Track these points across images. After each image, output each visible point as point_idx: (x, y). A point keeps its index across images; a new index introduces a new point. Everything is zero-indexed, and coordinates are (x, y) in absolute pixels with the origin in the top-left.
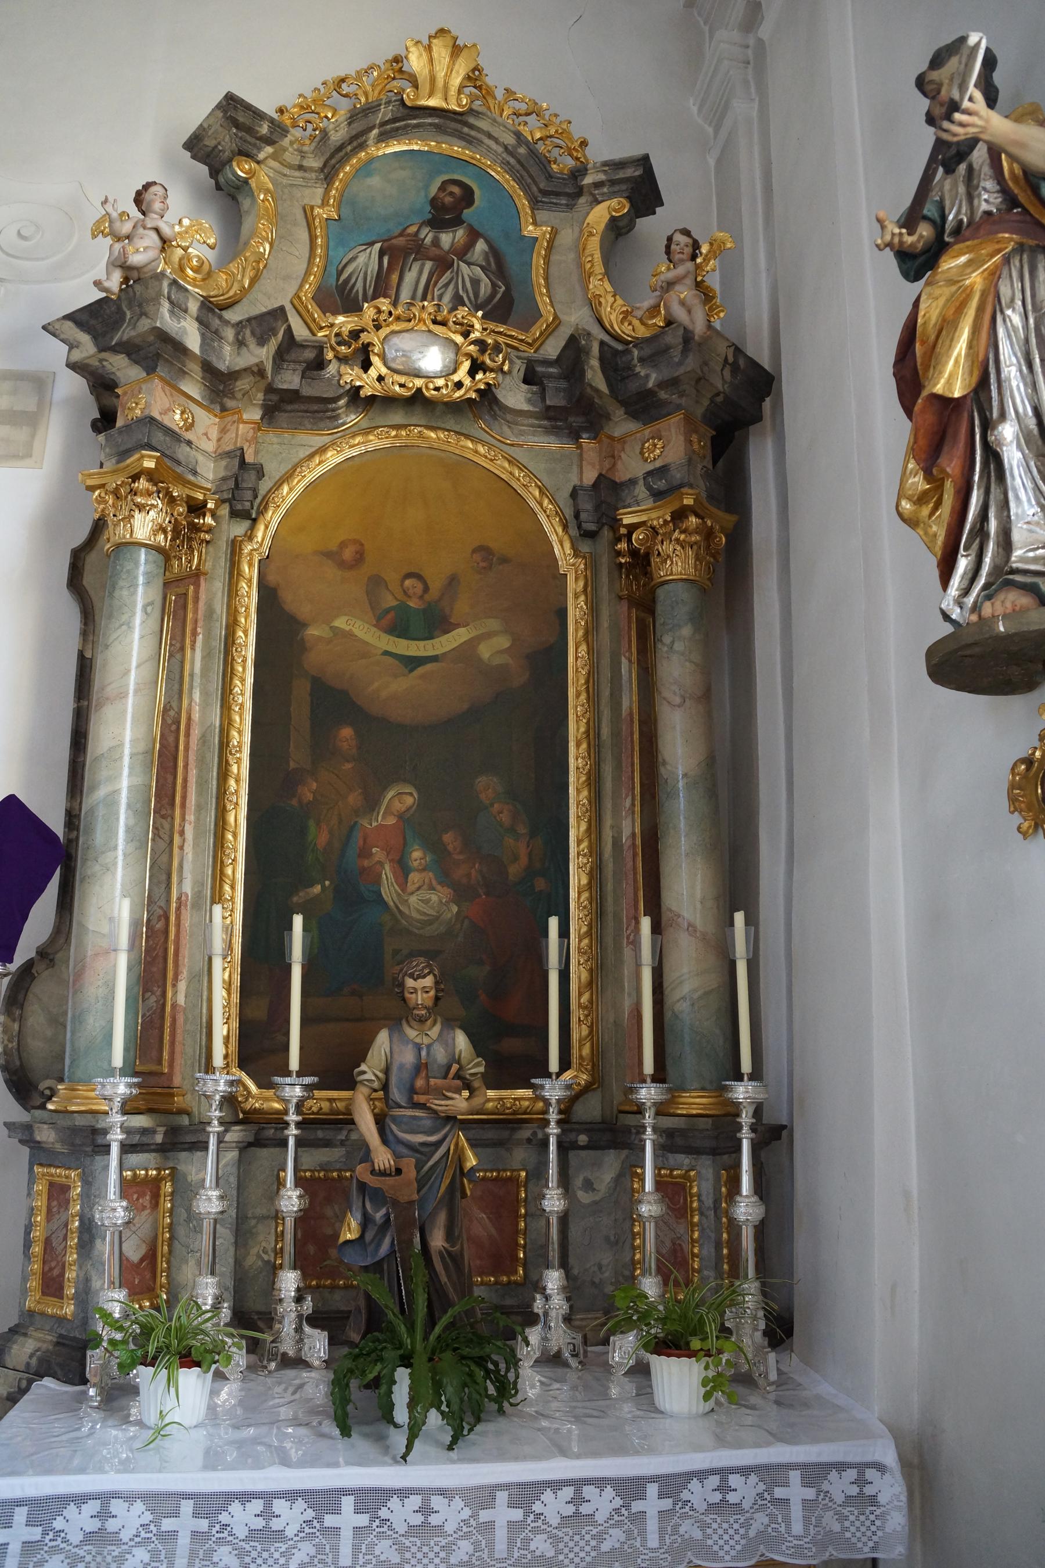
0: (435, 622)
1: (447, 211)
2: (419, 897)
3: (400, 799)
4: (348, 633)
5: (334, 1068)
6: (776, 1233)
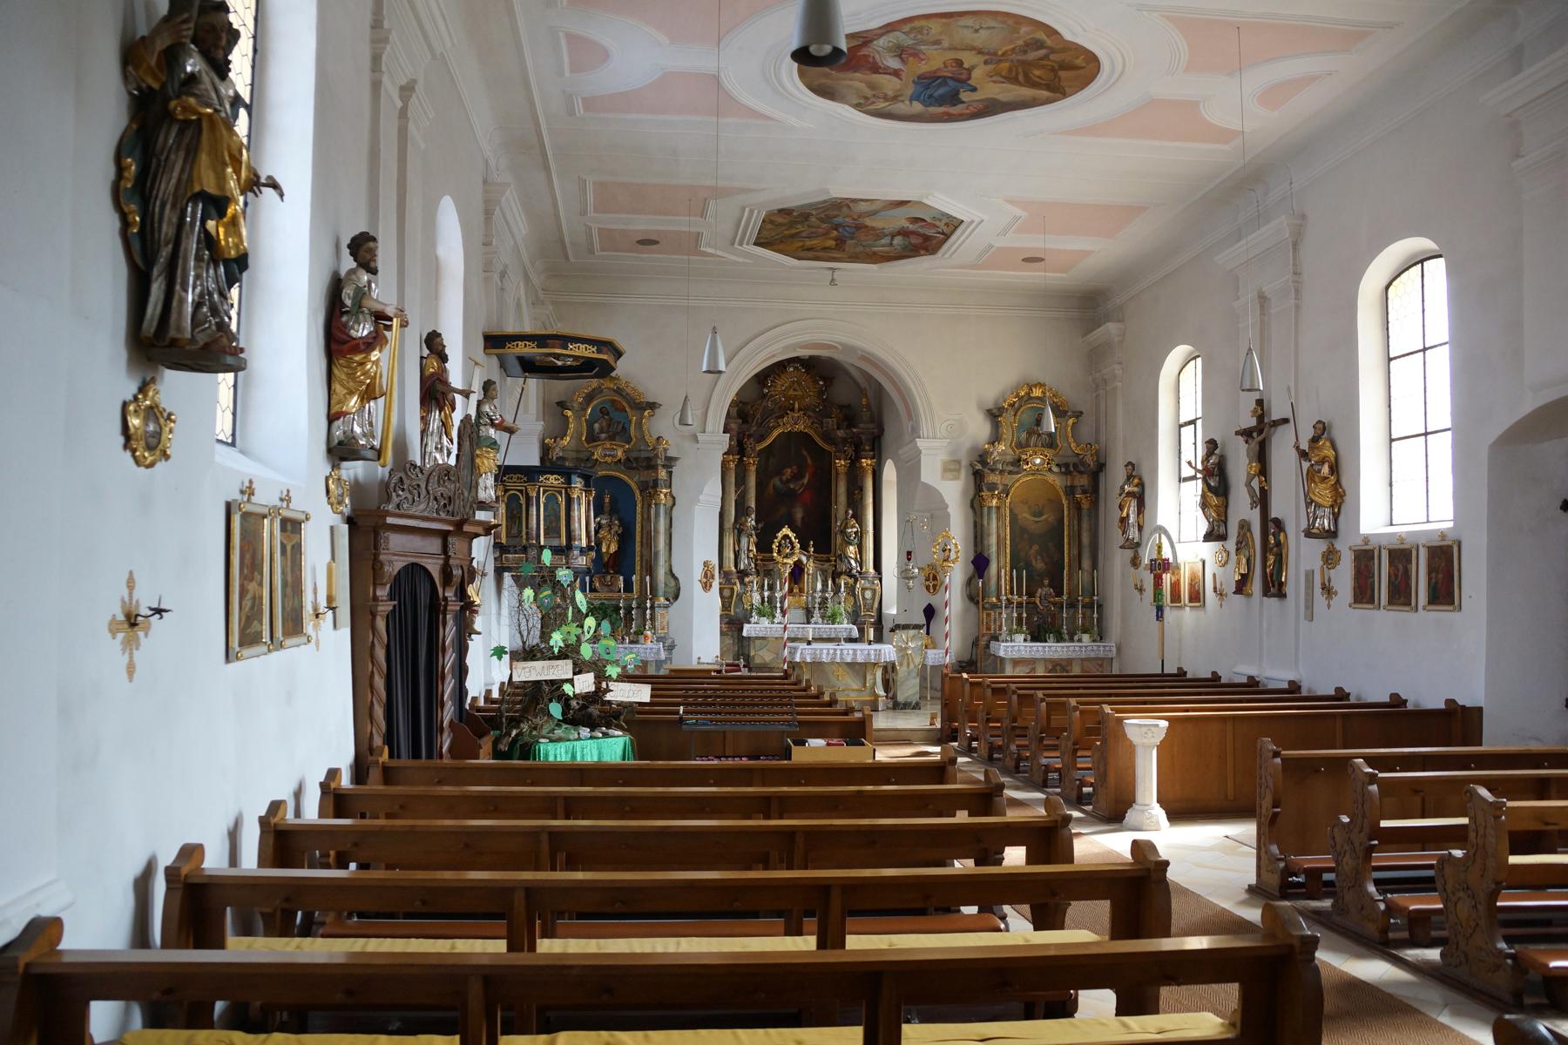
0: (1041, 514)
2: (1039, 565)
3: (1036, 547)
4: (1025, 516)
5: (1030, 594)
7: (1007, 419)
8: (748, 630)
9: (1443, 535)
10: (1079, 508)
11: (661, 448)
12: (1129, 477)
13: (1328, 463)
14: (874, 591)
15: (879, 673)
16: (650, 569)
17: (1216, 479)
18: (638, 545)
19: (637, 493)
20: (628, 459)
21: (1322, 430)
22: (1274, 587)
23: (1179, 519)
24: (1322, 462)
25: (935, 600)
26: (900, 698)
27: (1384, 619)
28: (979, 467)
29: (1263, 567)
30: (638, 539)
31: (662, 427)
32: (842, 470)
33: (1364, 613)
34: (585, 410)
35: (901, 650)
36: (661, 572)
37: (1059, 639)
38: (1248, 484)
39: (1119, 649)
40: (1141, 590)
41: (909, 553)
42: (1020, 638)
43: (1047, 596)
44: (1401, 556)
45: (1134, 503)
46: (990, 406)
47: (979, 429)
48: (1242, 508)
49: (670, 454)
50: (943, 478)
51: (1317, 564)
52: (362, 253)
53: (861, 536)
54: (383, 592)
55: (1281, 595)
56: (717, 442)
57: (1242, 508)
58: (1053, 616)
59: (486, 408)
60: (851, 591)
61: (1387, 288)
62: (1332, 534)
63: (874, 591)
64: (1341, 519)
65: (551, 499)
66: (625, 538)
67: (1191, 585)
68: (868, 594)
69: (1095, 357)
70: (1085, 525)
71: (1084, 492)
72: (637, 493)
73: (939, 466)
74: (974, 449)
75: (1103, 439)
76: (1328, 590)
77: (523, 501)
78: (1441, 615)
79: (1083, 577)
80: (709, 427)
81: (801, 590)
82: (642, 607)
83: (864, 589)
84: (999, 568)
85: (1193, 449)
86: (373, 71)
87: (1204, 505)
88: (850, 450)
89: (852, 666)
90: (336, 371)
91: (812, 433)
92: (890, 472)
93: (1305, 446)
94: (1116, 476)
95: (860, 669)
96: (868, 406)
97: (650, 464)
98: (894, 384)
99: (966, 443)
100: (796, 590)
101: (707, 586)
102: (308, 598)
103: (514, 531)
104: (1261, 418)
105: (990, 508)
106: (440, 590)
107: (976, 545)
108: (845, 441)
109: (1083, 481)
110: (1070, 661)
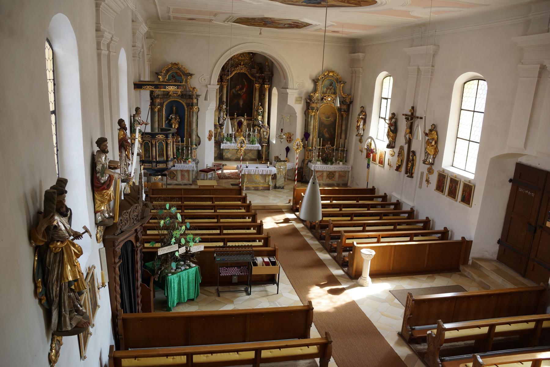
0: (329, 118)
1: (331, 85)
2: (327, 135)
3: (326, 129)
4: (324, 118)
6: (346, 156)
7: (320, 83)
8: (223, 146)
9: (470, 181)
10: (342, 116)
11: (194, 92)
12: (362, 112)
13: (435, 139)
14: (267, 132)
15: (270, 177)
16: (190, 136)
17: (393, 129)
18: (186, 126)
19: (186, 107)
20: (182, 95)
21: (434, 128)
22: (410, 173)
23: (378, 133)
24: (433, 139)
25: (290, 145)
26: (277, 185)
27: (444, 199)
28: (308, 101)
29: (407, 163)
30: (186, 124)
31: (195, 83)
32: (258, 88)
33: (438, 194)
34: (166, 75)
35: (279, 170)
36: (194, 137)
37: (332, 164)
38: (405, 136)
39: (352, 168)
40: (362, 151)
41: (282, 130)
42: (319, 163)
43: (329, 148)
44: (455, 182)
45: (362, 121)
46: (314, 77)
47: (310, 86)
48: (401, 141)
49: (198, 94)
50: (295, 103)
51: (426, 172)
52: (102, 146)
53: (263, 112)
54: (117, 260)
55: (411, 176)
56: (214, 86)
57: (401, 141)
58: (330, 154)
59: (137, 118)
60: (259, 132)
61: (465, 83)
62: (432, 164)
63: (267, 132)
64: (436, 159)
65: (161, 143)
66: (181, 123)
67: (380, 158)
68: (265, 133)
69: (353, 63)
70: (344, 123)
71: (345, 111)
72: (186, 107)
73: (294, 99)
74: (307, 93)
75: (353, 92)
76: (428, 181)
77: (150, 144)
78: (463, 206)
79: (342, 141)
80: (212, 83)
81: (241, 131)
82: (187, 147)
83: (263, 132)
84: (314, 137)
85: (386, 112)
86: (98, 49)
87: (388, 135)
88: (261, 81)
89: (262, 175)
90: (96, 196)
91: (247, 73)
92: (275, 91)
93: (427, 132)
94: (356, 109)
95: (264, 176)
96: (268, 66)
97: (191, 97)
98: (281, 69)
99: (304, 91)
100: (240, 131)
101: (210, 139)
102: (96, 285)
103: (147, 155)
104: (412, 114)
105: (311, 116)
106: (135, 244)
107: (305, 127)
108: (259, 77)
109: (345, 107)
110: (335, 172)
